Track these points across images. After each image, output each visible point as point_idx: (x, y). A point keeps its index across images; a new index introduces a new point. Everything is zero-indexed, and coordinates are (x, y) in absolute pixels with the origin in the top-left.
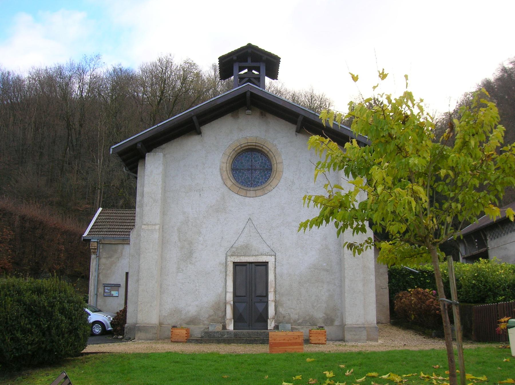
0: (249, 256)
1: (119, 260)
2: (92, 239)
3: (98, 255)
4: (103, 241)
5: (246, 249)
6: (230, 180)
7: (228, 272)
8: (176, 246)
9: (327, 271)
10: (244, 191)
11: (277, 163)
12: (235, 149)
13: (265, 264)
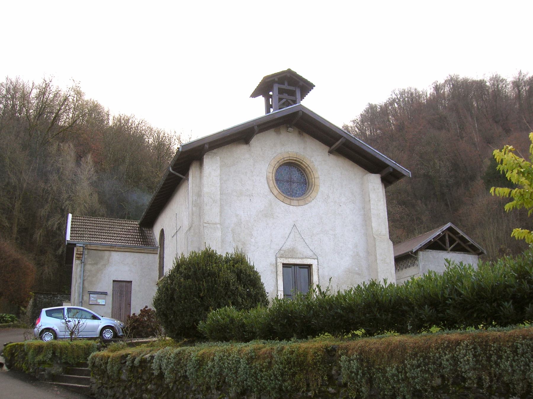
0: (296, 258)
1: (105, 267)
2: (78, 244)
3: (83, 261)
4: (89, 247)
5: (292, 252)
6: (276, 189)
7: (278, 273)
8: (231, 246)
9: (359, 274)
10: (289, 200)
11: (314, 178)
12: (279, 161)
13: (309, 266)
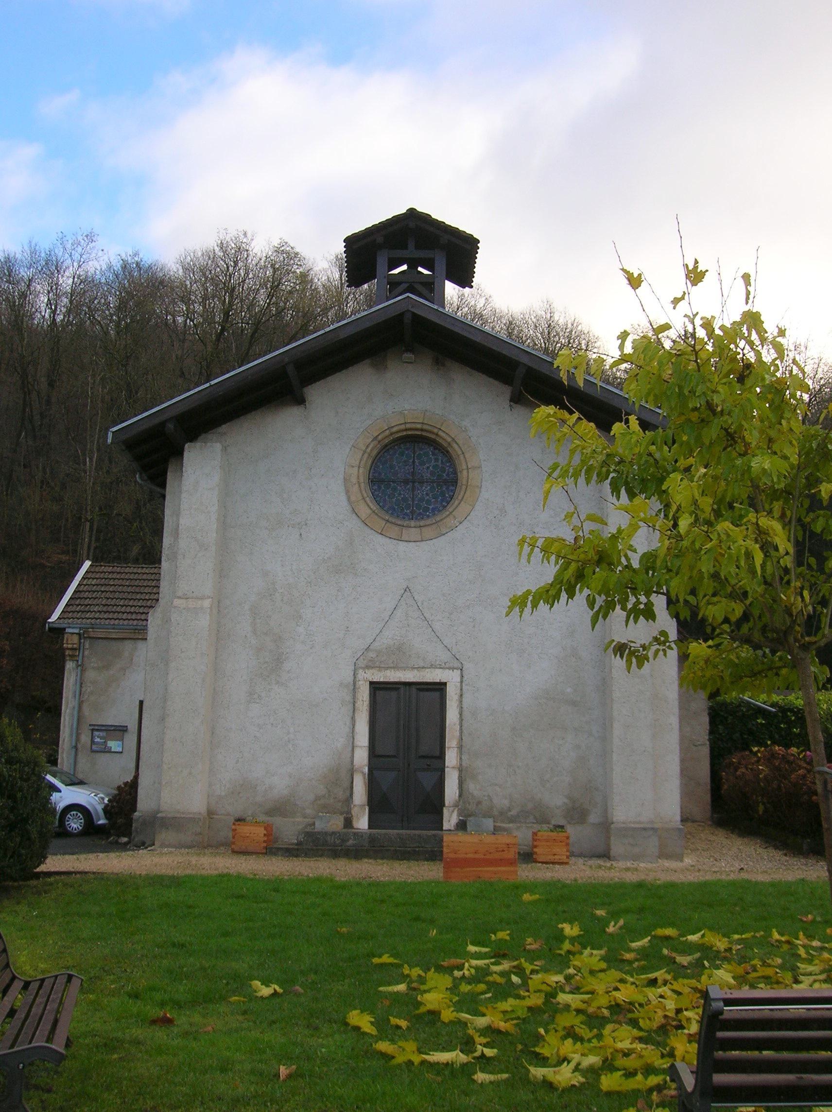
2: (69, 627)
3: (80, 663)
7: (359, 704)
9: (574, 703)
10: (397, 528)
11: (468, 469)
13: (440, 687)
